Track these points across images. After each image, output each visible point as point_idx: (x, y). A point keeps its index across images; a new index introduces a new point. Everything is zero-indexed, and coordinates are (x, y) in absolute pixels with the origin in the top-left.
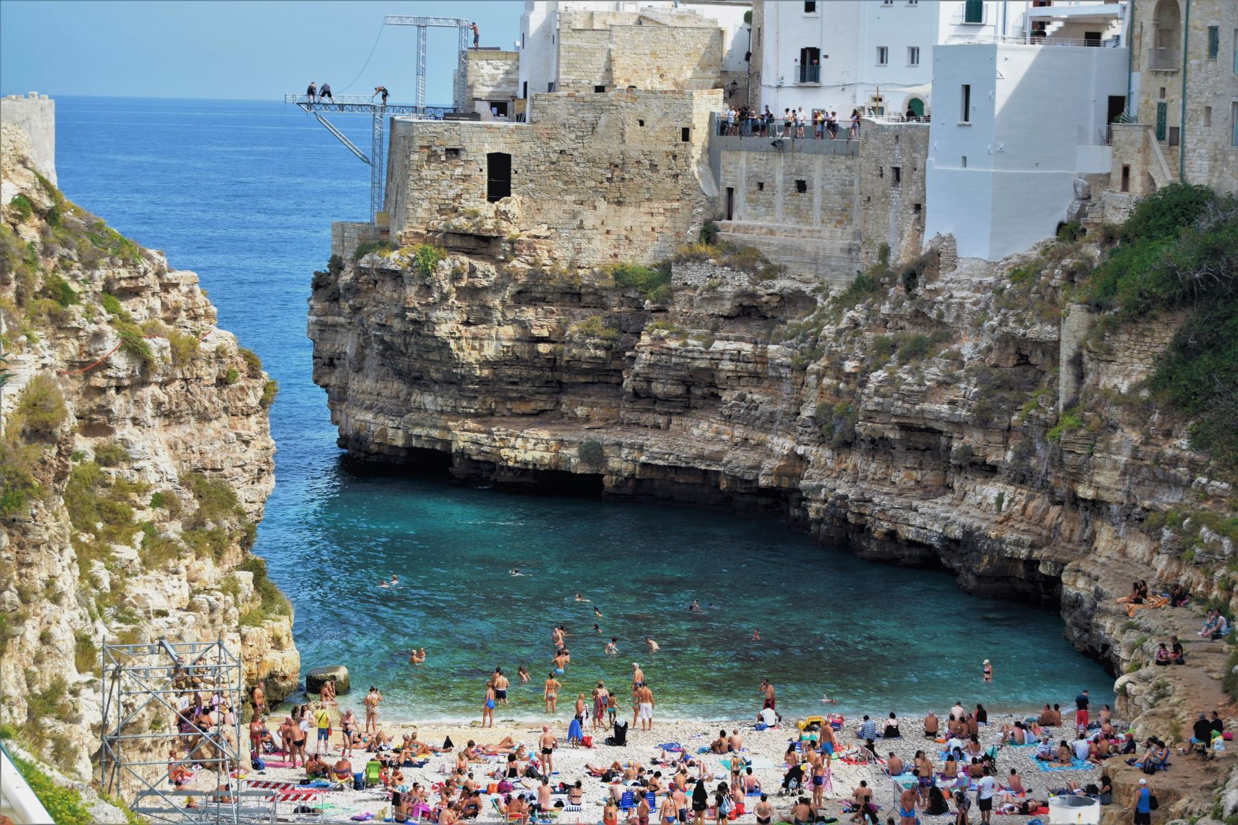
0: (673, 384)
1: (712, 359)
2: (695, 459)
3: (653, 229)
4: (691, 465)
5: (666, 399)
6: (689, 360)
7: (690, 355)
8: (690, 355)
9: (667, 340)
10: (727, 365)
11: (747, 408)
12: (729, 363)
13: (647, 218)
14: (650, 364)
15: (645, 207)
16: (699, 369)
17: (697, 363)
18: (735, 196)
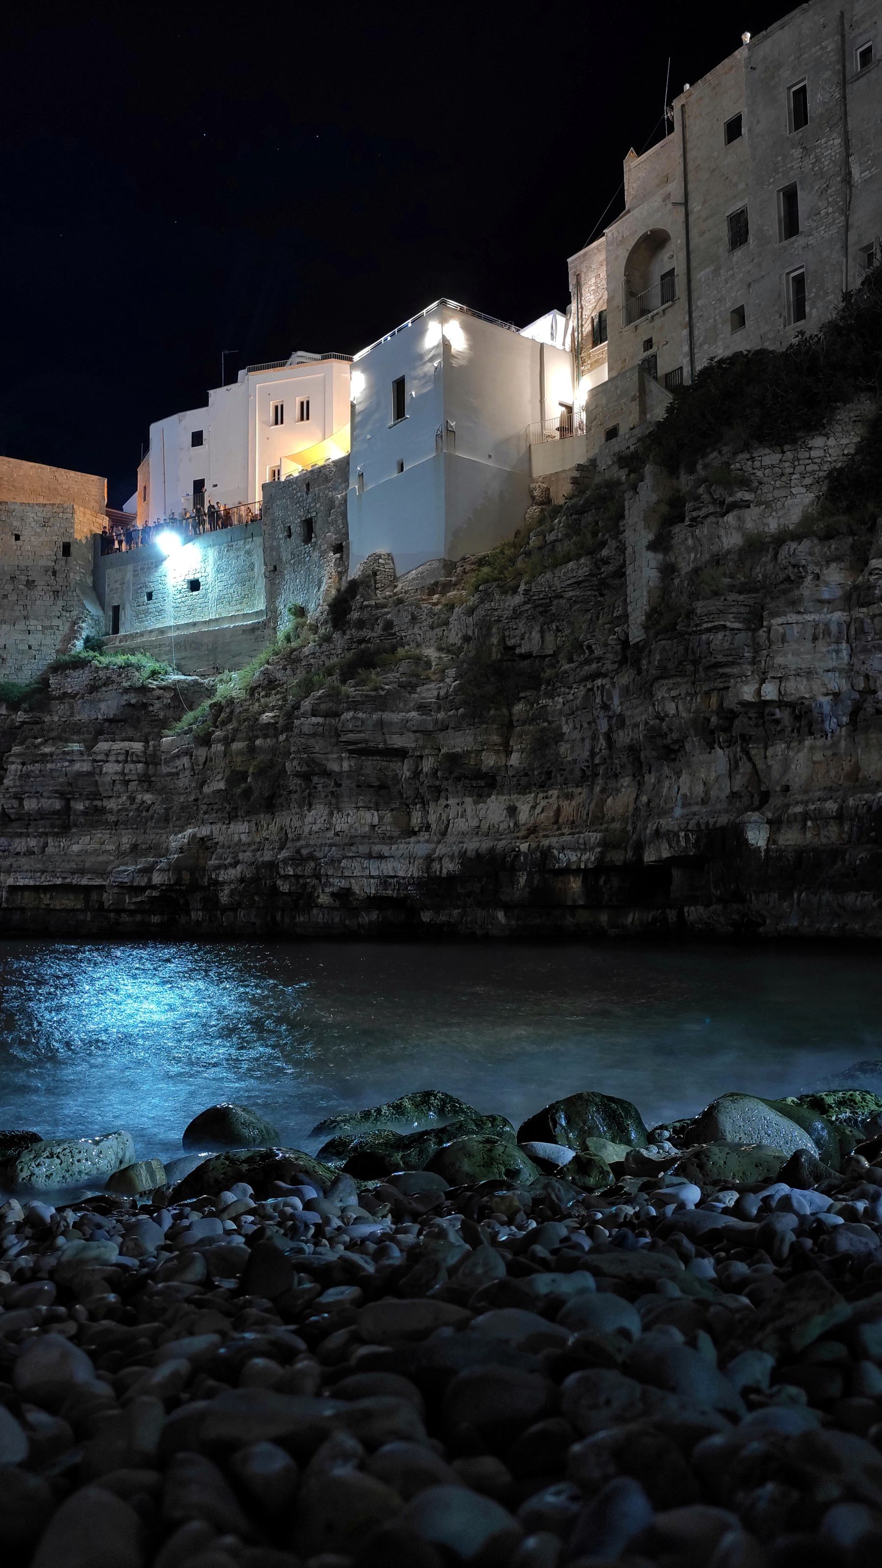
0: (49, 798)
1: (95, 761)
2: (73, 873)
3: (30, 647)
4: (68, 881)
5: (42, 815)
6: (67, 764)
7: (68, 758)
8: (68, 758)
9: (42, 747)
10: (111, 768)
11: (137, 809)
12: (116, 764)
13: (26, 636)
14: (21, 776)
15: (21, 626)
16: (80, 774)
17: (77, 767)
18: (122, 613)
